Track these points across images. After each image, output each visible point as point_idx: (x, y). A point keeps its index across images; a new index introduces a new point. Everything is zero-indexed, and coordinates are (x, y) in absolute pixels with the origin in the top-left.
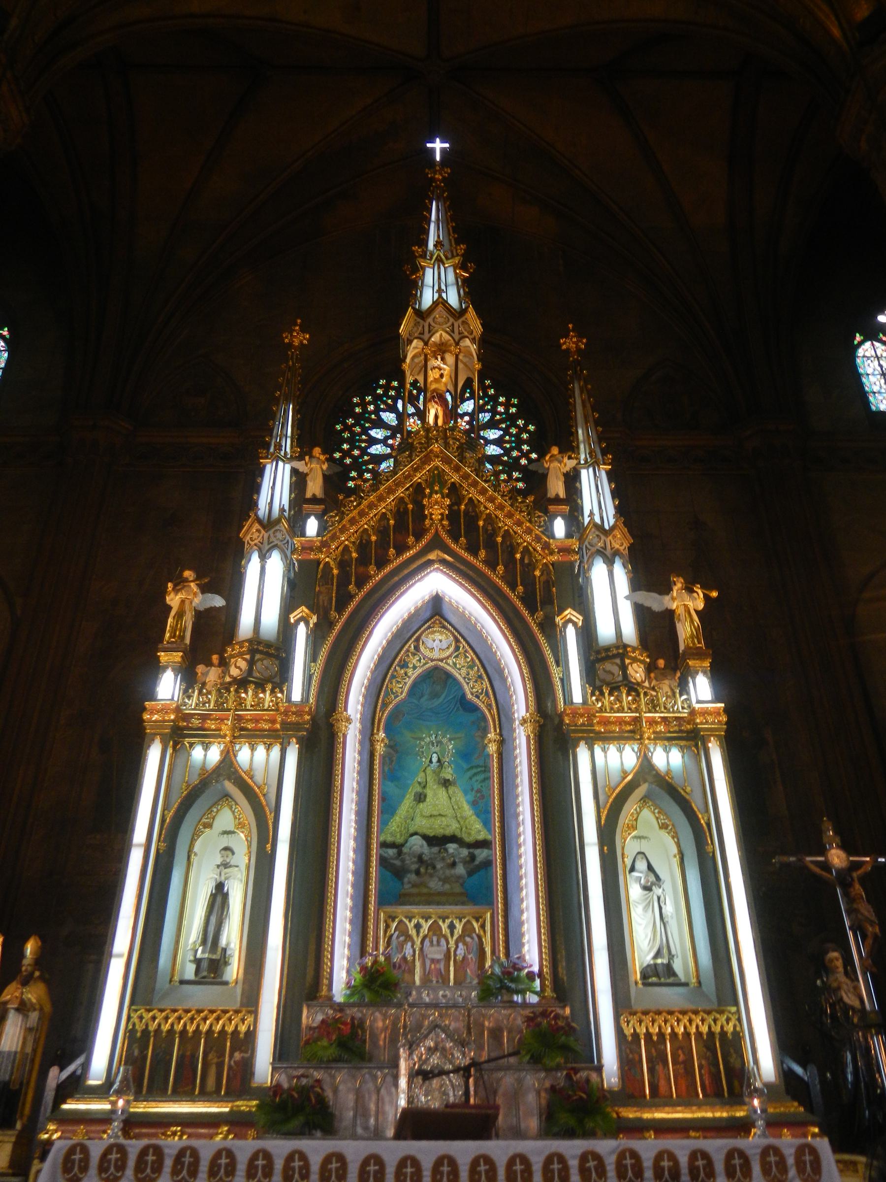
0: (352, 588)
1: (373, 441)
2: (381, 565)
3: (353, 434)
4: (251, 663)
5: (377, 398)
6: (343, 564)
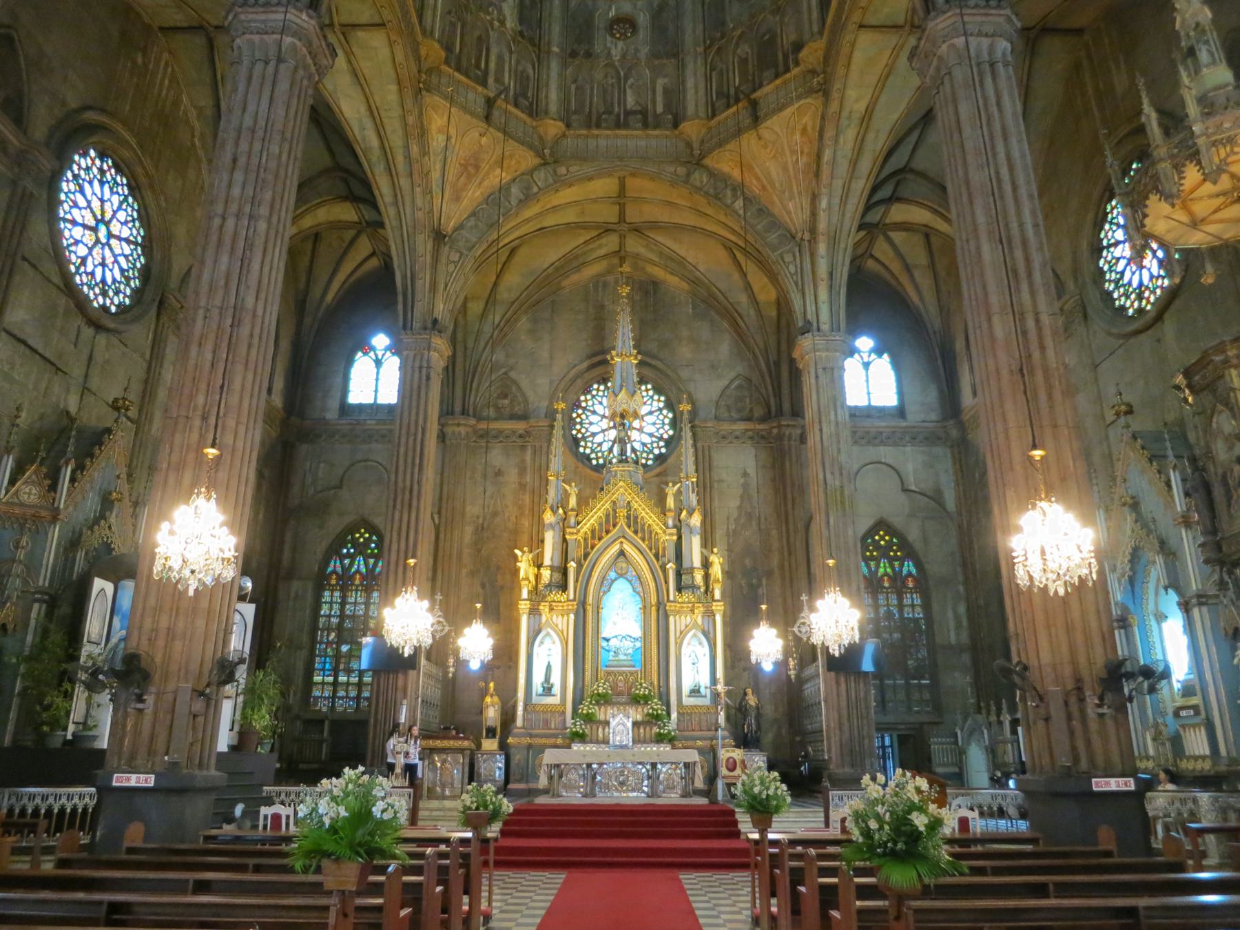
0: (589, 550)
1: (591, 423)
2: (600, 539)
3: (582, 420)
4: (551, 576)
5: (593, 397)
6: (585, 540)
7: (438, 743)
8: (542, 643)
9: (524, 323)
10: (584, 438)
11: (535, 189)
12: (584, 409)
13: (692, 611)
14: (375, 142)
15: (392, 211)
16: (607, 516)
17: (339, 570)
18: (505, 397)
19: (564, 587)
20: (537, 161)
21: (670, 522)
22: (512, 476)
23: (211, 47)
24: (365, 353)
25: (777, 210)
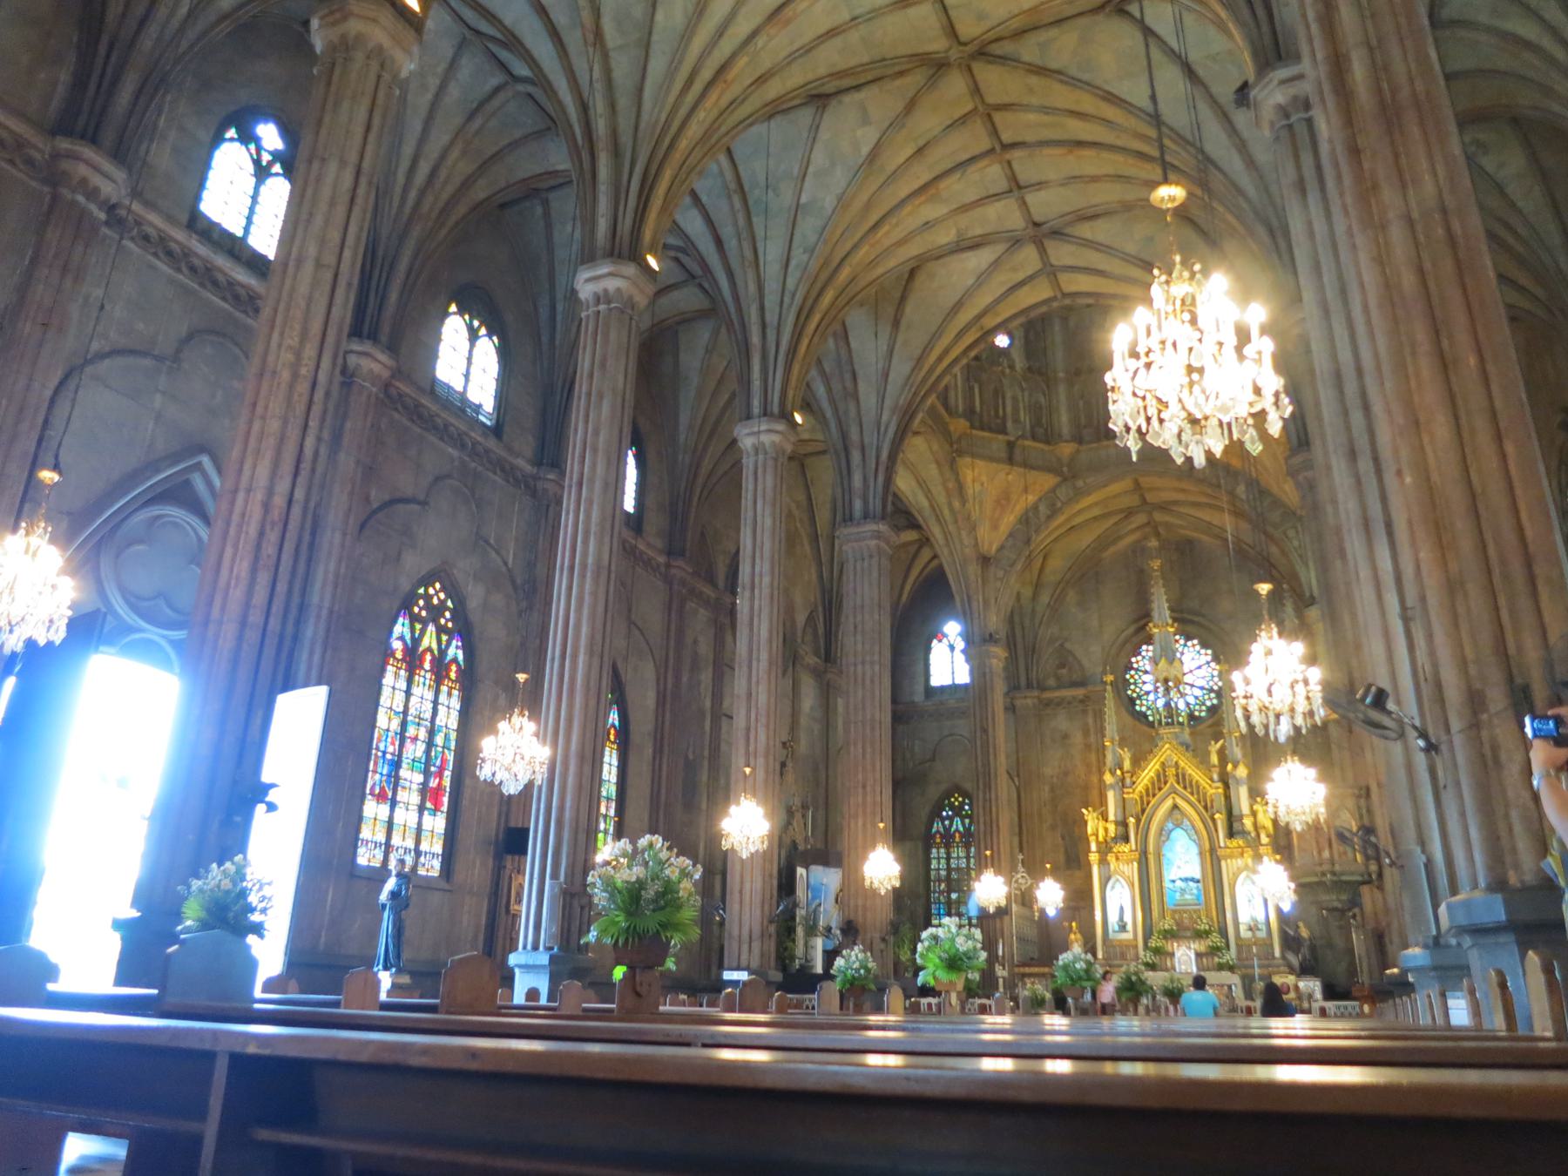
2: (1154, 795)
6: (1141, 797)
7: (1027, 970)
8: (1113, 887)
9: (1072, 596)
10: (1139, 697)
11: (1059, 505)
12: (1137, 670)
13: (1242, 855)
14: (925, 503)
15: (946, 551)
16: (1158, 776)
17: (942, 830)
18: (1062, 666)
19: (1126, 839)
20: (1057, 480)
21: (1215, 777)
22: (1077, 738)
23: (803, 466)
24: (940, 641)
25: (1275, 490)
